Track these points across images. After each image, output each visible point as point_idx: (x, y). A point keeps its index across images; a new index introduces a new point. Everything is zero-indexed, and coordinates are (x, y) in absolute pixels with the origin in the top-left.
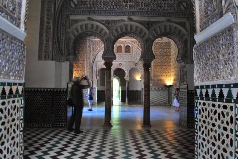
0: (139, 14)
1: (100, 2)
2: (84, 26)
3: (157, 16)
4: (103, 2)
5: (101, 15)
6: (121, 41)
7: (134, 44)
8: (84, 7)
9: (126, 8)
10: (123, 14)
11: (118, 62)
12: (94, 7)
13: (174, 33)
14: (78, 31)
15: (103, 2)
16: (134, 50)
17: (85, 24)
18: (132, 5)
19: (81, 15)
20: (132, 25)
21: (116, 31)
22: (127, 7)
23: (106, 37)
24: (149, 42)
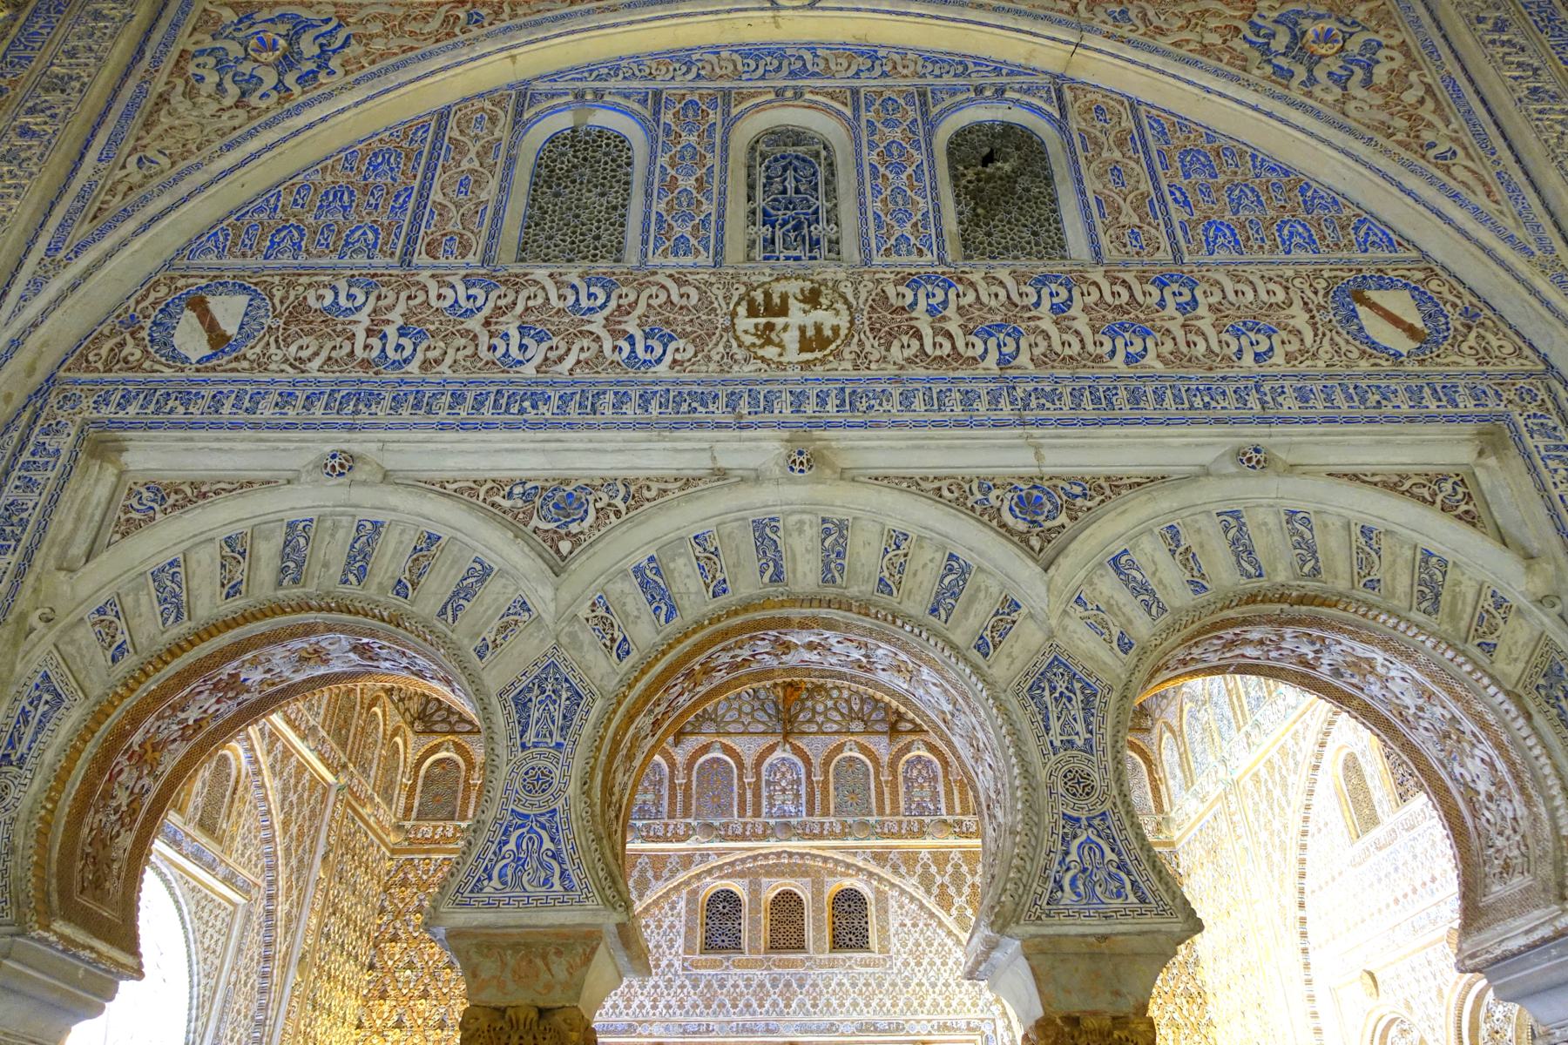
0: (918, 404)
1: (499, 311)
2: (268, 551)
3: (1124, 422)
4: (527, 309)
5: (488, 426)
6: (791, 855)
7: (896, 880)
8: (305, 354)
9: (763, 359)
10: (732, 406)
11: (768, 1031)
12: (419, 356)
13: (1361, 594)
14: (174, 605)
15: (519, 308)
16: (894, 925)
17: (292, 525)
18: (828, 332)
19: (256, 426)
20: (842, 526)
21: (645, 585)
22: (780, 345)
23: (526, 649)
24: (1076, 709)
